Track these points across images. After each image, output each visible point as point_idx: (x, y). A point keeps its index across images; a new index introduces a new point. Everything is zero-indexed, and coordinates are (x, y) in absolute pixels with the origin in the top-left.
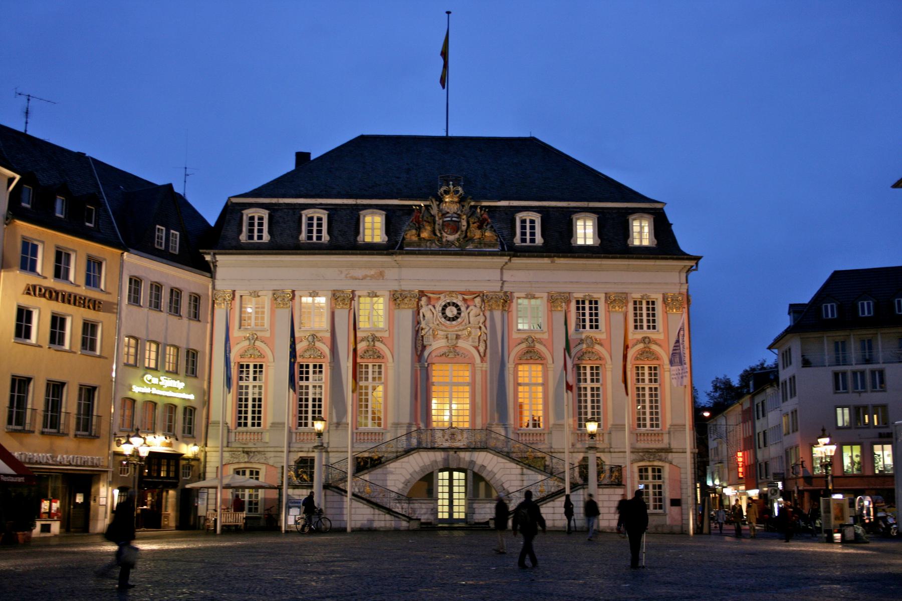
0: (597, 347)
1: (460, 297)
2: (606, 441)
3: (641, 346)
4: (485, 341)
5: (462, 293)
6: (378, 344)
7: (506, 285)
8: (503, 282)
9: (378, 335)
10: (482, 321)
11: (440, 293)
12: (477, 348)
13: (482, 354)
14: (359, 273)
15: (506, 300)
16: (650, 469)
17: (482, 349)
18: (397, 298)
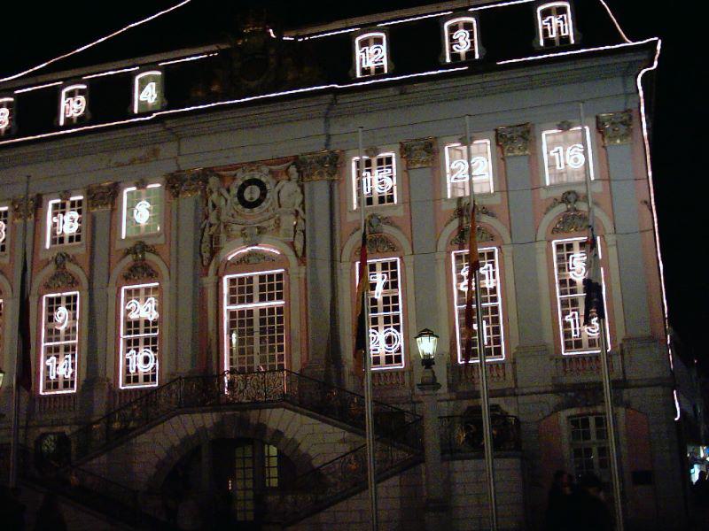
0: (485, 219)
1: (265, 169)
2: (510, 376)
3: (563, 208)
4: (304, 232)
5: (266, 163)
6: (150, 257)
7: (334, 140)
8: (329, 137)
9: (149, 242)
10: (299, 200)
11: (235, 167)
12: (292, 245)
13: (300, 254)
14: (124, 156)
15: (333, 164)
16: (592, 420)
17: (299, 246)
18: (174, 184)
